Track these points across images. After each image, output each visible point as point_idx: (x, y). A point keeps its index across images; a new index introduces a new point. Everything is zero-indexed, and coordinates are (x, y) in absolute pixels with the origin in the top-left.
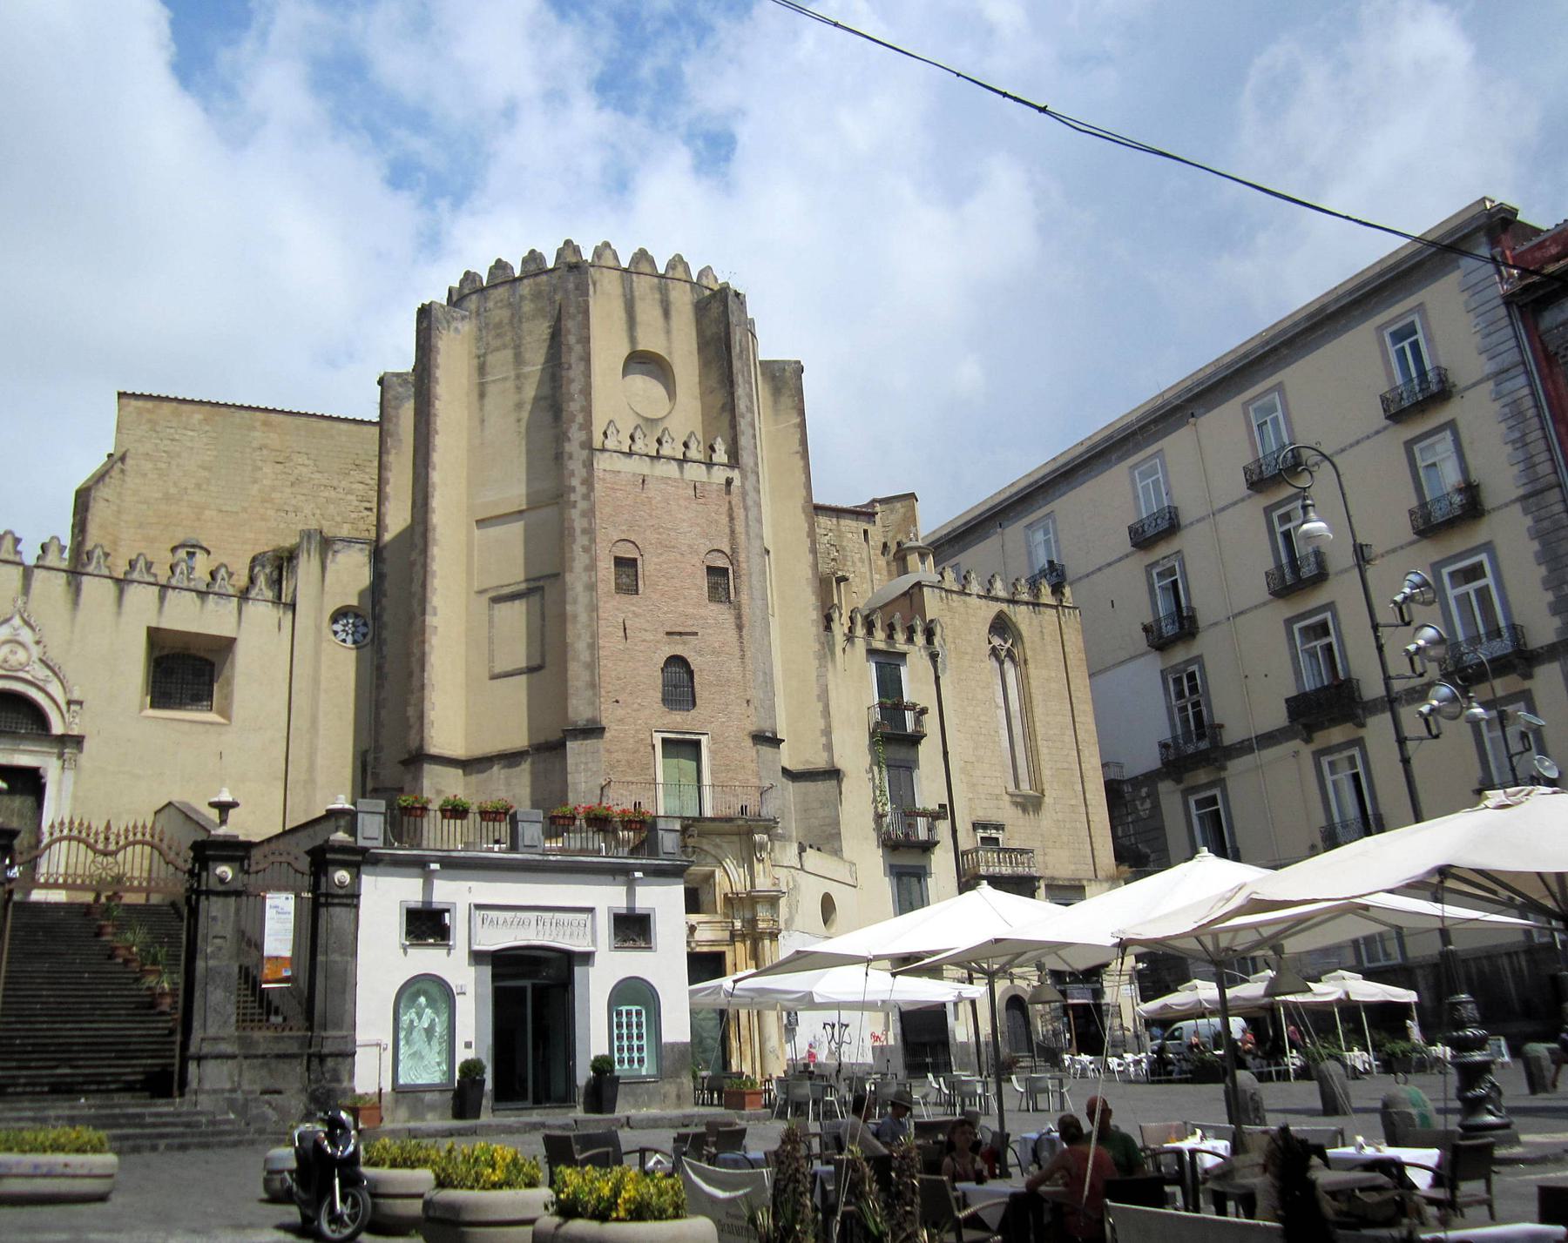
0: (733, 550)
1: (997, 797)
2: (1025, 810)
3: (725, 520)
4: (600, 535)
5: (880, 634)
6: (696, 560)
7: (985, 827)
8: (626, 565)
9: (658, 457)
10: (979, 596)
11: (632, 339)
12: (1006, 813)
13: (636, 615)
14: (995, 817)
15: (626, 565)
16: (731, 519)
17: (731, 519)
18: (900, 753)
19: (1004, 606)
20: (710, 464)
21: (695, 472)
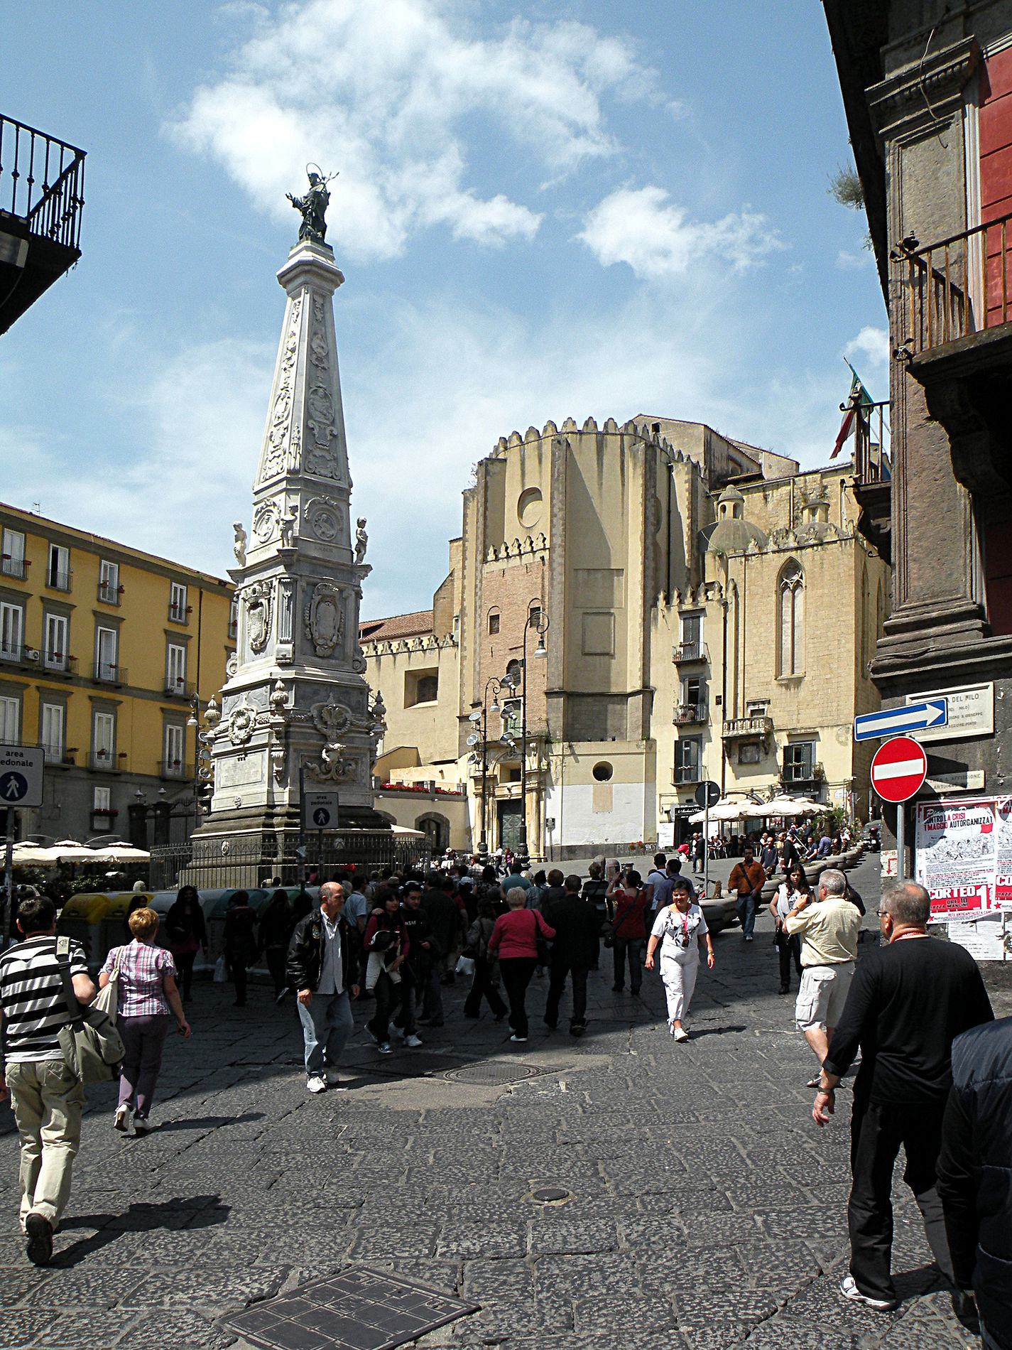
0: (543, 596)
1: (768, 683)
2: (787, 687)
3: (539, 580)
4: (484, 607)
5: (689, 600)
6: (525, 608)
7: (754, 704)
8: (495, 619)
9: (508, 557)
10: (774, 552)
11: (523, 485)
12: (774, 691)
13: (497, 643)
14: (763, 697)
15: (495, 619)
16: (543, 578)
17: (543, 578)
18: (695, 670)
19: (793, 554)
20: (533, 552)
21: (527, 559)
